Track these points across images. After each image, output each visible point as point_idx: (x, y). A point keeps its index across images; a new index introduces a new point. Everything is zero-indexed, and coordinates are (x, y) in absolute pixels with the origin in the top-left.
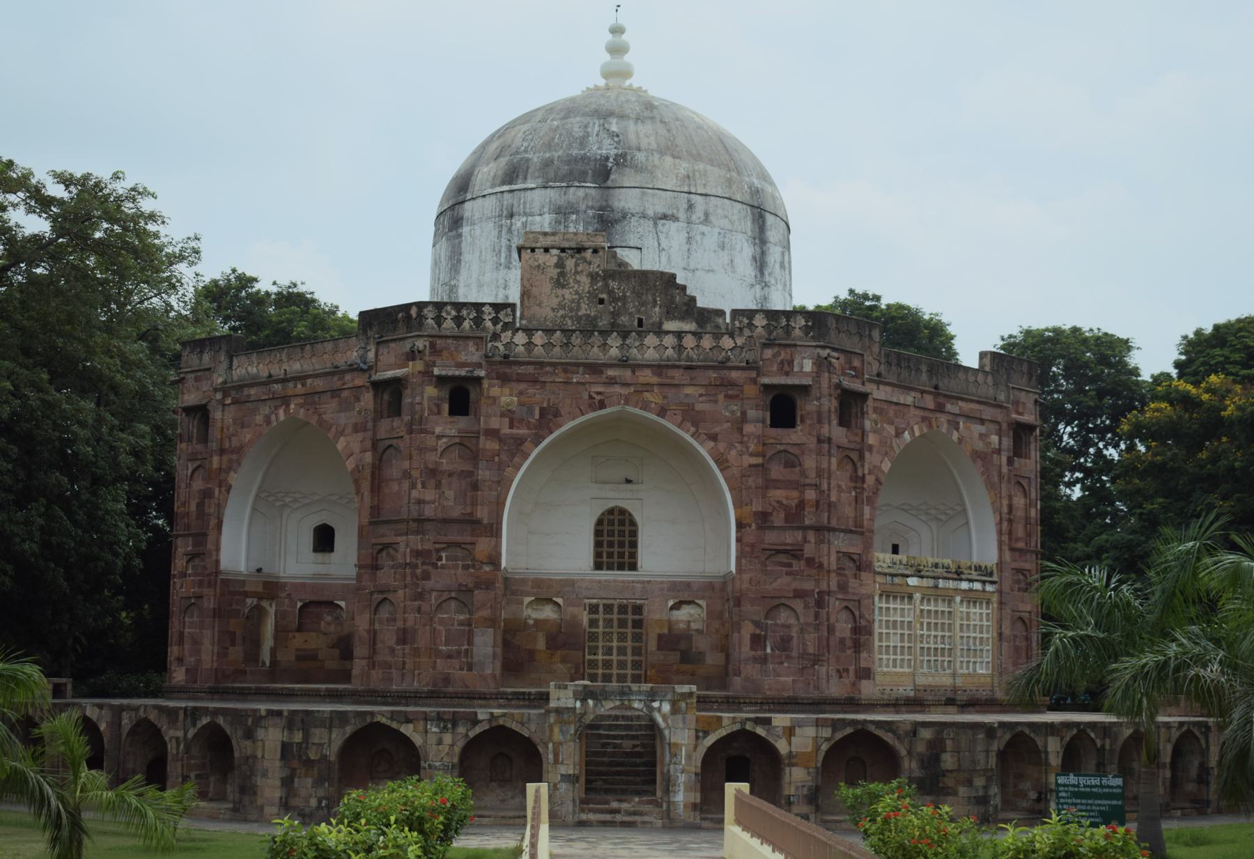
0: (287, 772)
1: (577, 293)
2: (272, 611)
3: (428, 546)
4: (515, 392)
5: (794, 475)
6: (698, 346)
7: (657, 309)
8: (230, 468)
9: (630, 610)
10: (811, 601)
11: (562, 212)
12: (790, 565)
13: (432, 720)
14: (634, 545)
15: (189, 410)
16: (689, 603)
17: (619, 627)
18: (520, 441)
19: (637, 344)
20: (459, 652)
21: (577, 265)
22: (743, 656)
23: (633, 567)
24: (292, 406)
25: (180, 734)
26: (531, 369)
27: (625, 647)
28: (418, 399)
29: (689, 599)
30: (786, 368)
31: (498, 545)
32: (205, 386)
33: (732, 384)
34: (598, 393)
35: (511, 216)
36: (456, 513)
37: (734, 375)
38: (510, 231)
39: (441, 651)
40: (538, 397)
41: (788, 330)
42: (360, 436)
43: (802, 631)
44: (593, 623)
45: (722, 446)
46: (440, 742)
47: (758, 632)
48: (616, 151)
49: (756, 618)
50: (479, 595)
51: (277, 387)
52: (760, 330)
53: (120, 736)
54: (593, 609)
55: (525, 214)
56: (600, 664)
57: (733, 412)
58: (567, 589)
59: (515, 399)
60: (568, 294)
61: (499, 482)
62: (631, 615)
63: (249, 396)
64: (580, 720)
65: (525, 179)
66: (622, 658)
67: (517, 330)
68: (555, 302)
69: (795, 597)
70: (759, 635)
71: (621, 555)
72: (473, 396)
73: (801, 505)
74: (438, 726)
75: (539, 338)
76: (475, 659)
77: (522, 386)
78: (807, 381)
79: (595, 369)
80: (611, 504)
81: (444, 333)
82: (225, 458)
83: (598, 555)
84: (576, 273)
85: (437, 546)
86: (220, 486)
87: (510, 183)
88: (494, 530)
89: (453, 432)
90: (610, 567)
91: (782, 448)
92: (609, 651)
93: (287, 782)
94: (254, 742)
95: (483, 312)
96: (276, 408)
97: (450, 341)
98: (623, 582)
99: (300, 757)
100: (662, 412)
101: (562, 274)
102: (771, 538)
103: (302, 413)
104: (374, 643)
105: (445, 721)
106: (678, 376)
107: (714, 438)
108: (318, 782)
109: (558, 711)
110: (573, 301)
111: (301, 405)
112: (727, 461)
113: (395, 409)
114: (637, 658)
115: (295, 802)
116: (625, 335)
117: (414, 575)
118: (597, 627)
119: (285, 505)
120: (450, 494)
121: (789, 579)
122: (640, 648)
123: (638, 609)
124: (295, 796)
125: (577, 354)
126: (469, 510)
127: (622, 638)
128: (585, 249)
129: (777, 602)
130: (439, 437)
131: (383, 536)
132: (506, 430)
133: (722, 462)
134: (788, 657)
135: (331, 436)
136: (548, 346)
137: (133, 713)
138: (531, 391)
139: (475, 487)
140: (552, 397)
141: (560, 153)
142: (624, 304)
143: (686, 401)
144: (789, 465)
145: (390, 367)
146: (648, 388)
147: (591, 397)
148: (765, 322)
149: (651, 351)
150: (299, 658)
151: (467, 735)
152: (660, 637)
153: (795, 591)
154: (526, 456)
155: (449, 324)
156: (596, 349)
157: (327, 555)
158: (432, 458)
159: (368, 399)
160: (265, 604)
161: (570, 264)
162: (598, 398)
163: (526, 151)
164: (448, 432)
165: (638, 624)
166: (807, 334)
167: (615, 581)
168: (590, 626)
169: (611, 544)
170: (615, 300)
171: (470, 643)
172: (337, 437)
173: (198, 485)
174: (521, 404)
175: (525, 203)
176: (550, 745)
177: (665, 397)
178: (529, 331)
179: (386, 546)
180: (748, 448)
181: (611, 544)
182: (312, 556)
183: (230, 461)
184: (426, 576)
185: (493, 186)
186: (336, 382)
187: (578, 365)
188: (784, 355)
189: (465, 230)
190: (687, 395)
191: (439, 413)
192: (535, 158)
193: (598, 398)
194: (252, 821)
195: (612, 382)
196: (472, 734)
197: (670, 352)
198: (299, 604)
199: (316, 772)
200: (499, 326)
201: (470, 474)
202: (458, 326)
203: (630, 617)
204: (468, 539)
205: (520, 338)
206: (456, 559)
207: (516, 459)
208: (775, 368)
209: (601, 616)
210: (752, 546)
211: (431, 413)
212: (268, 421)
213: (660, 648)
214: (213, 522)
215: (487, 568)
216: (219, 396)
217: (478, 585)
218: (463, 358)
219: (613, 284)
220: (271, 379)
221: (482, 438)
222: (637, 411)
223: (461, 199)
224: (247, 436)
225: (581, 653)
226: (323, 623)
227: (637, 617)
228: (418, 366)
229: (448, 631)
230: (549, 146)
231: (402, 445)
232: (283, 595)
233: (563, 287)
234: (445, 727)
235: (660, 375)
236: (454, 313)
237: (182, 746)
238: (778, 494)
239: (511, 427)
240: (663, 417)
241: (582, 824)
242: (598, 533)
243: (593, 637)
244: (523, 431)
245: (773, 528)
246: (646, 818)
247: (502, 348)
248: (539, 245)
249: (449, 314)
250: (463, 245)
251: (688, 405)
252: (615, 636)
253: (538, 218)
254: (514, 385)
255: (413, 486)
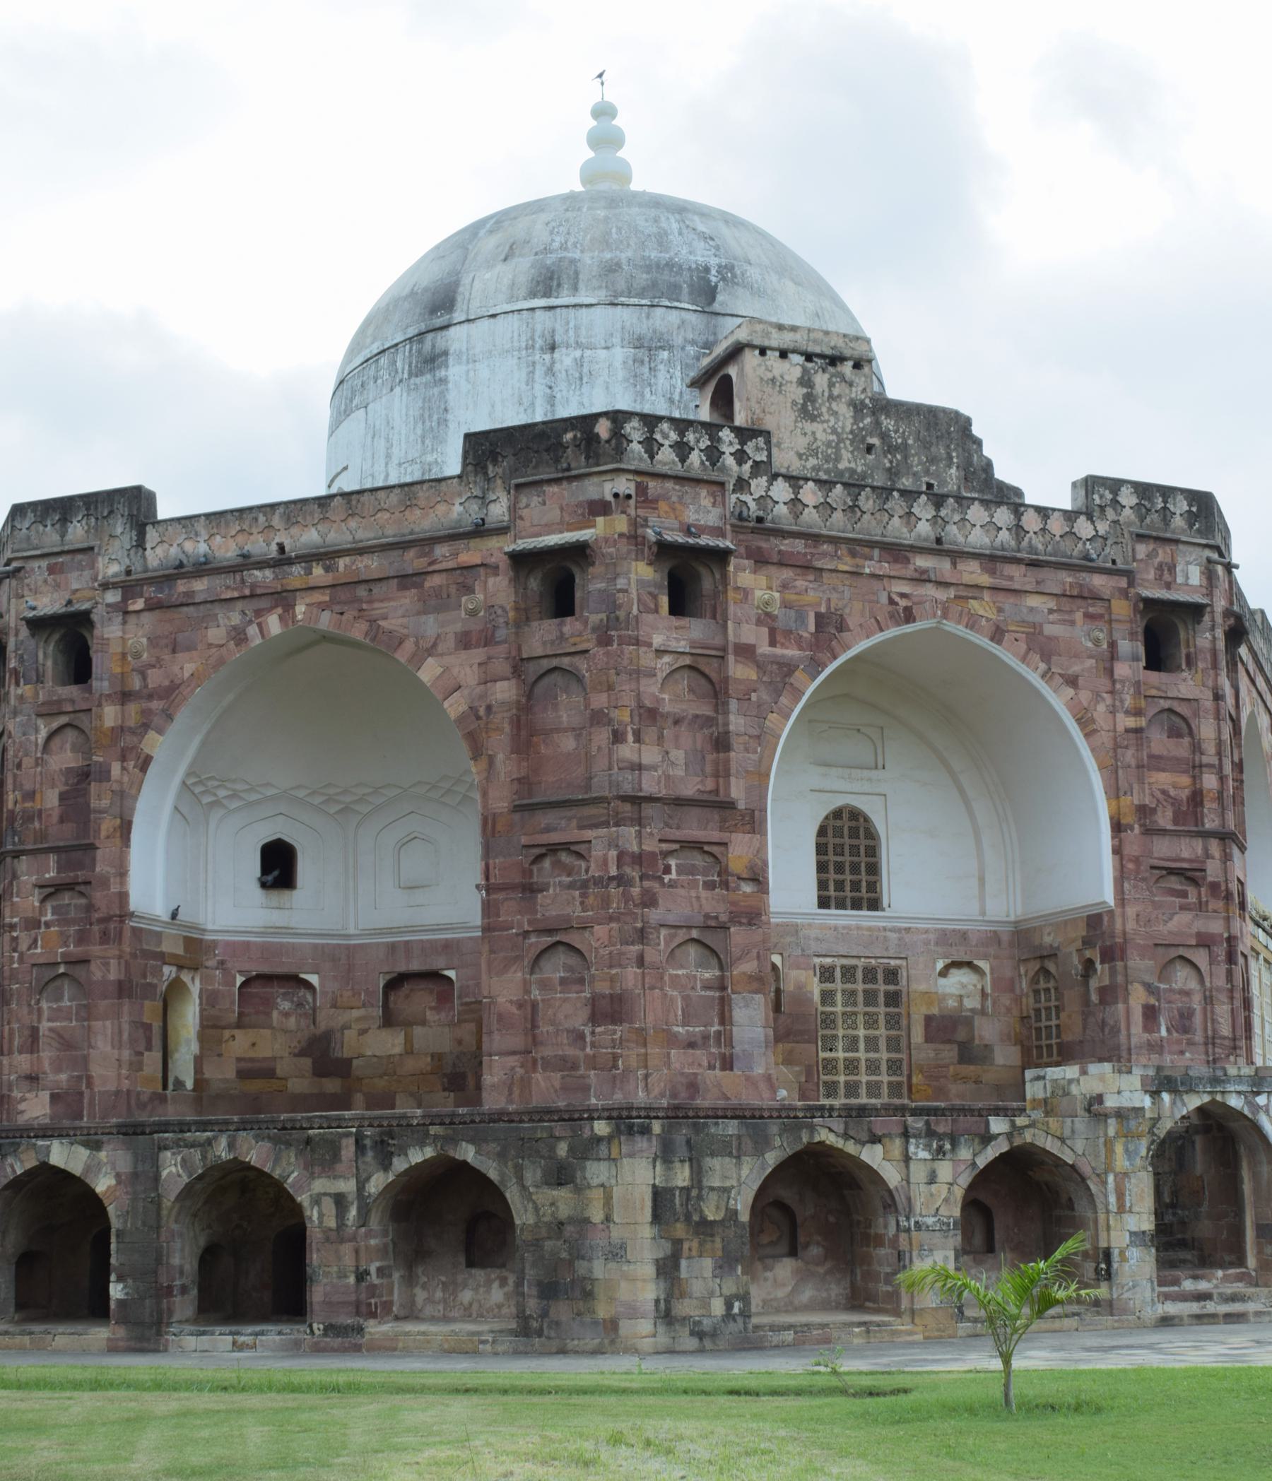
0: (666, 1248)
1: (834, 431)
2: (195, 988)
3: (650, 846)
4: (775, 584)
5: (1181, 748)
6: (1043, 530)
7: (953, 471)
8: (146, 726)
9: (880, 977)
10: (1221, 951)
11: (647, 348)
12: (1184, 895)
13: (916, 1136)
14: (874, 869)
15: (38, 625)
16: (969, 964)
17: (866, 1004)
18: (787, 668)
19: (957, 518)
20: (706, 1037)
21: (831, 385)
22: (1134, 1041)
23: (875, 905)
24: (300, 609)
25: (347, 1186)
26: (799, 546)
27: (876, 1038)
28: (621, 583)
29: (967, 959)
30: (1167, 577)
31: (763, 846)
32: (77, 581)
33: (1096, 598)
34: (903, 595)
35: (553, 348)
36: (690, 789)
37: (1098, 581)
38: (550, 371)
39: (675, 1035)
40: (813, 595)
41: (1166, 514)
42: (478, 654)
43: (1209, 1000)
44: (827, 997)
45: (1085, 696)
46: (932, 1179)
47: (1152, 1001)
48: (717, 261)
49: (1148, 978)
50: (738, 934)
51: (264, 576)
52: (1127, 512)
53: (157, 1202)
54: (827, 974)
55: (578, 345)
56: (841, 1066)
57: (1097, 642)
58: (788, 939)
59: (777, 595)
60: (820, 431)
61: (758, 737)
62: (883, 985)
63: (190, 594)
64: (1151, 1132)
65: (575, 288)
66: (872, 1055)
67: (775, 476)
68: (801, 443)
69: (1197, 946)
70: (1153, 1006)
71: (856, 886)
72: (707, 584)
73: (1197, 798)
74: (928, 1147)
75: (810, 494)
76: (737, 1049)
77: (787, 574)
78: (1198, 598)
79: (896, 552)
80: (839, 801)
81: (660, 468)
82: (133, 708)
83: (822, 885)
84: (831, 397)
85: (665, 846)
86: (123, 759)
87: (547, 294)
88: (753, 822)
89: (683, 646)
90: (841, 905)
91: (1165, 704)
92: (852, 1044)
93: (668, 1268)
94: (578, 1190)
95: (719, 440)
96: (259, 613)
97: (669, 485)
98: (870, 929)
99: (688, 1217)
100: (998, 635)
101: (810, 398)
102: (1163, 849)
103: (325, 621)
104: (534, 1026)
105: (940, 1137)
106: (1018, 576)
107: (1072, 681)
108: (725, 1264)
109: (1120, 1114)
110: (829, 444)
111: (323, 607)
112: (1093, 721)
113: (562, 602)
114: (894, 1055)
115: (684, 1308)
116: (938, 501)
117: (627, 898)
118: (833, 1004)
119: (216, 803)
120: (678, 755)
121: (1186, 917)
122: (898, 1038)
123: (892, 975)
124: (682, 1295)
125: (870, 526)
126: (710, 785)
127: (871, 1022)
128: (842, 359)
129: (1174, 953)
130: (660, 652)
131: (548, 830)
132: (764, 649)
133: (1085, 721)
134: (1191, 1043)
135: (402, 656)
136: (826, 507)
137: (197, 1155)
138: (801, 584)
139: (722, 743)
140: (834, 596)
141: (629, 254)
142: (906, 457)
143: (1030, 618)
144: (1174, 733)
145: (549, 529)
146: (976, 593)
147: (892, 602)
148: (1134, 500)
149: (977, 531)
150: (243, 1075)
151: (974, 1164)
152: (929, 1019)
153: (1199, 935)
154: (798, 693)
155: (666, 455)
156: (896, 521)
157: (286, 894)
158: (650, 688)
159: (498, 590)
160: (186, 977)
161: (821, 380)
162: (903, 603)
163: (564, 247)
164: (673, 645)
165: (893, 999)
166: (1191, 526)
167: (859, 928)
168: (823, 1003)
169: (839, 868)
170: (890, 449)
171: (725, 1018)
172: (419, 658)
173: (65, 758)
174: (786, 605)
175: (577, 328)
176: (1111, 1178)
177: (1000, 610)
178: (794, 481)
179: (553, 849)
180: (1122, 701)
181: (839, 868)
182: (258, 892)
183: (146, 713)
184: (650, 900)
185: (511, 299)
186: (412, 561)
187: (871, 544)
188: (1163, 554)
189: (454, 372)
190: (1031, 609)
191: (656, 611)
192: (589, 261)
193: (903, 603)
194: (577, 1353)
195: (922, 578)
196: (982, 1162)
197: (1004, 536)
198: (240, 980)
199: (718, 1244)
200: (747, 467)
201: (709, 721)
202: (683, 461)
203: (882, 987)
204: (715, 835)
205: (781, 491)
206: (692, 870)
207: (784, 700)
208: (1151, 575)
209: (838, 985)
210: (1136, 860)
211: (644, 609)
212: (239, 636)
213: (928, 1039)
214: (108, 825)
215: (747, 888)
216: (112, 597)
217: (735, 918)
218: (691, 516)
219: (888, 423)
220: (246, 562)
221: (731, 658)
222: (960, 630)
223: (438, 322)
224: (187, 666)
225: (813, 1047)
226: (275, 1014)
227: (891, 988)
228: (620, 524)
229: (686, 998)
230: (605, 242)
231: (582, 664)
232: (211, 963)
233: (813, 418)
234: (940, 1150)
235: (992, 572)
236: (674, 436)
237: (353, 1212)
238: (1162, 779)
239: (773, 643)
240: (999, 642)
241: (1166, 1322)
242: (821, 849)
243: (828, 1021)
244: (791, 652)
245: (1163, 832)
246: (1251, 1307)
247: (752, 505)
248: (774, 344)
249: (666, 436)
250: (452, 396)
251: (1034, 625)
252: (860, 1019)
253: (602, 354)
254: (773, 570)
255: (618, 737)
